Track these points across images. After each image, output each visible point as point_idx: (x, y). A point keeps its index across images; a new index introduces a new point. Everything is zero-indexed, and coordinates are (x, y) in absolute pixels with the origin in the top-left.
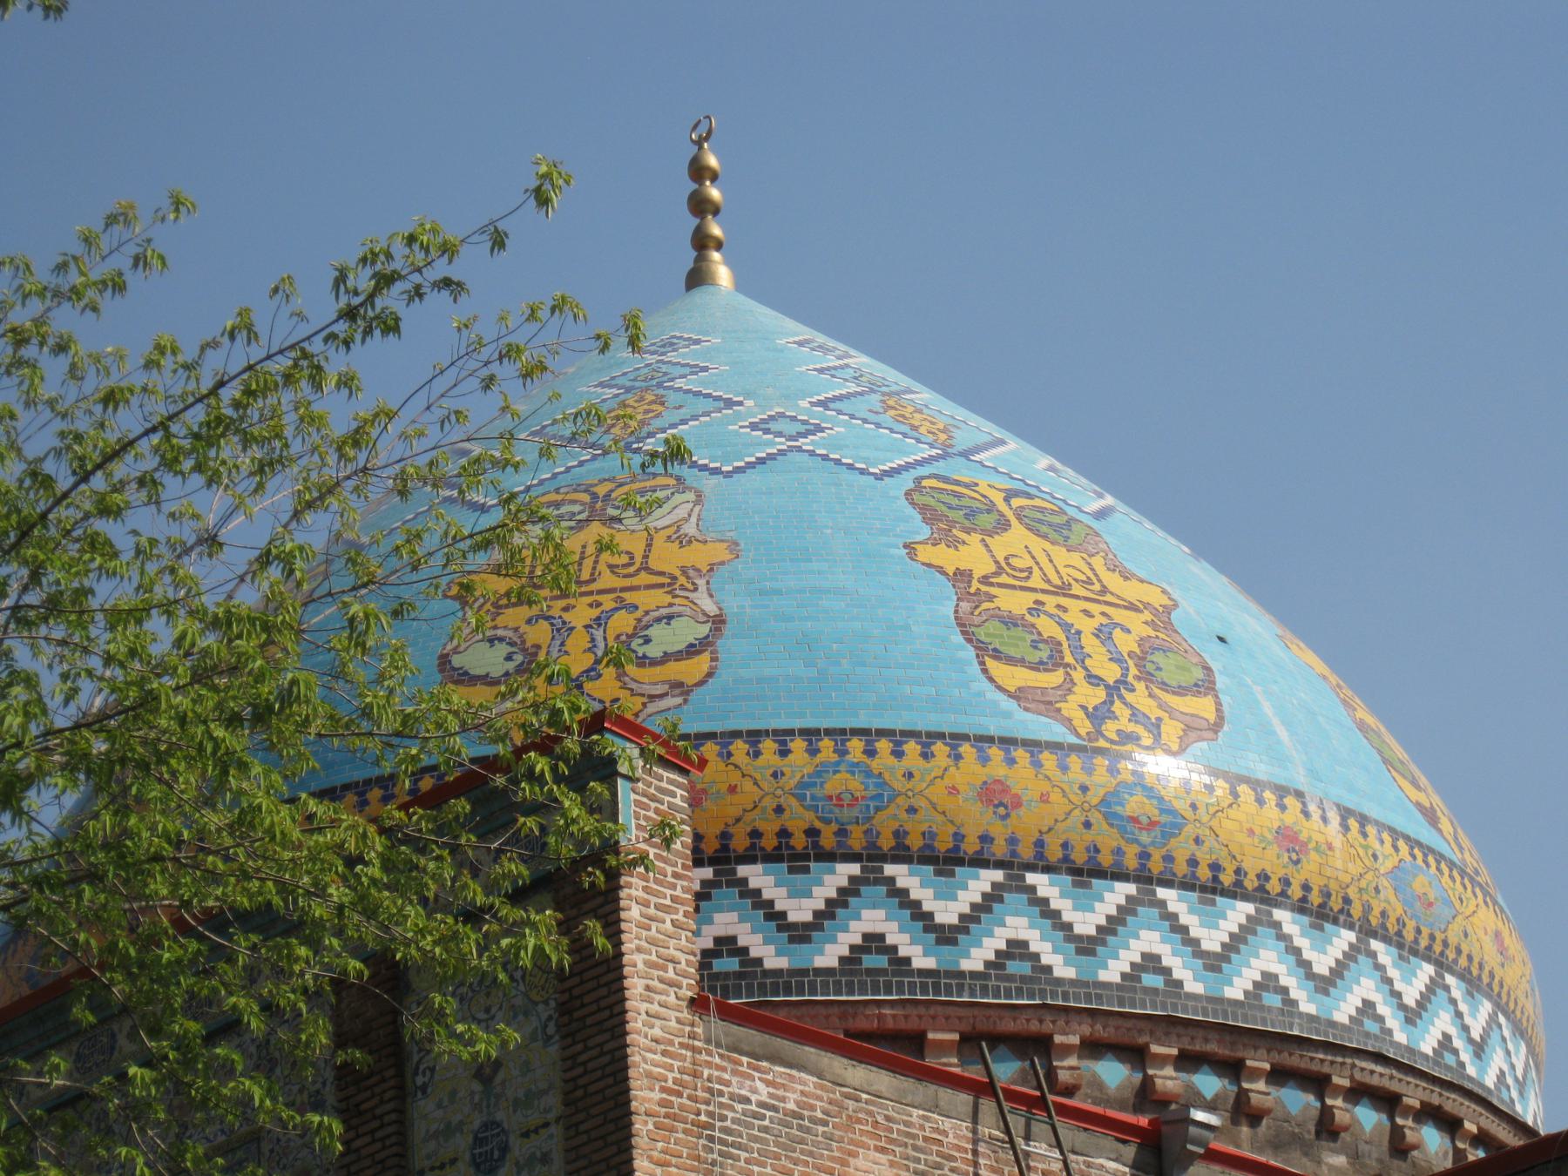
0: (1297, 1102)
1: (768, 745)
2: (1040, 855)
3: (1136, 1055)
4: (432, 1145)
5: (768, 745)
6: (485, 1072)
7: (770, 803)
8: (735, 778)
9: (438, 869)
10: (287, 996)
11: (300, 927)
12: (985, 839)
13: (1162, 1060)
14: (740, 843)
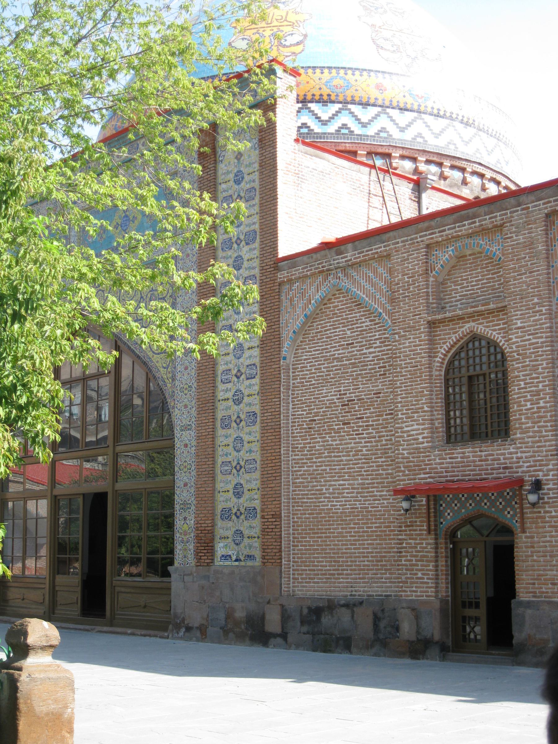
0: (457, 175)
1: (318, 71)
2: (391, 104)
3: (414, 160)
4: (223, 176)
5: (318, 71)
6: (239, 155)
7: (318, 87)
8: (308, 79)
9: (228, 98)
10: (187, 133)
11: (189, 115)
12: (376, 99)
13: (421, 161)
14: (309, 97)
